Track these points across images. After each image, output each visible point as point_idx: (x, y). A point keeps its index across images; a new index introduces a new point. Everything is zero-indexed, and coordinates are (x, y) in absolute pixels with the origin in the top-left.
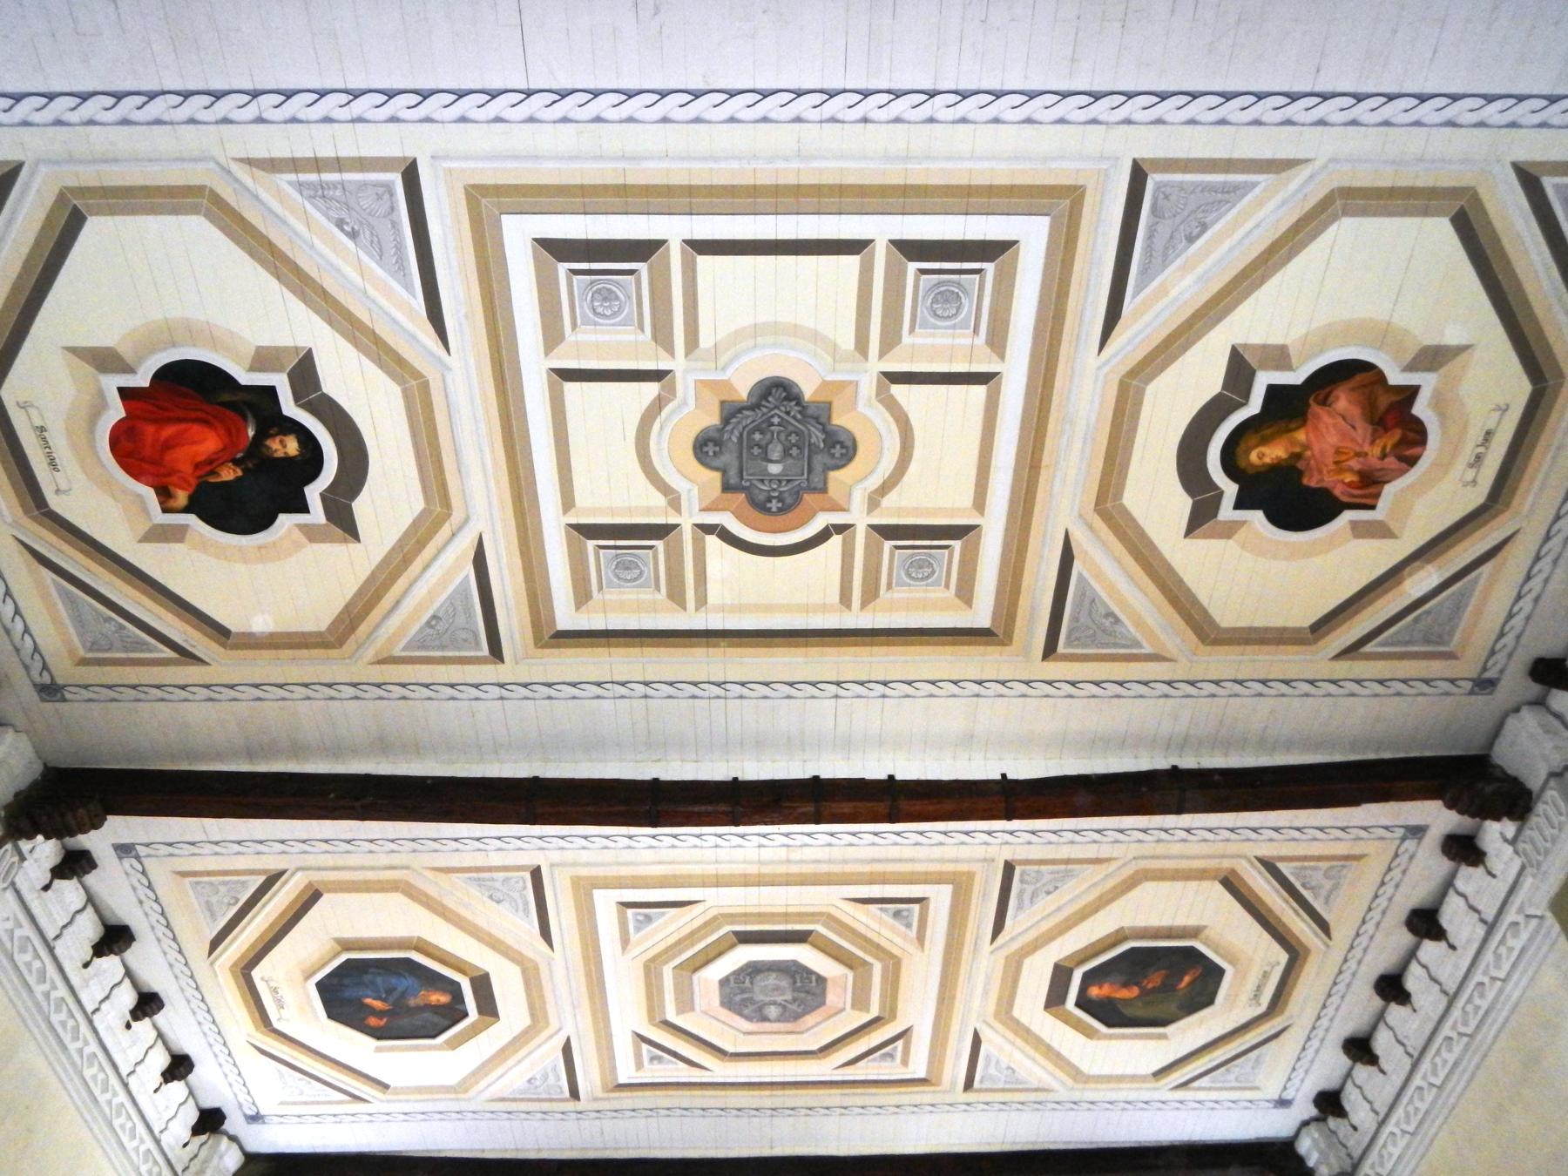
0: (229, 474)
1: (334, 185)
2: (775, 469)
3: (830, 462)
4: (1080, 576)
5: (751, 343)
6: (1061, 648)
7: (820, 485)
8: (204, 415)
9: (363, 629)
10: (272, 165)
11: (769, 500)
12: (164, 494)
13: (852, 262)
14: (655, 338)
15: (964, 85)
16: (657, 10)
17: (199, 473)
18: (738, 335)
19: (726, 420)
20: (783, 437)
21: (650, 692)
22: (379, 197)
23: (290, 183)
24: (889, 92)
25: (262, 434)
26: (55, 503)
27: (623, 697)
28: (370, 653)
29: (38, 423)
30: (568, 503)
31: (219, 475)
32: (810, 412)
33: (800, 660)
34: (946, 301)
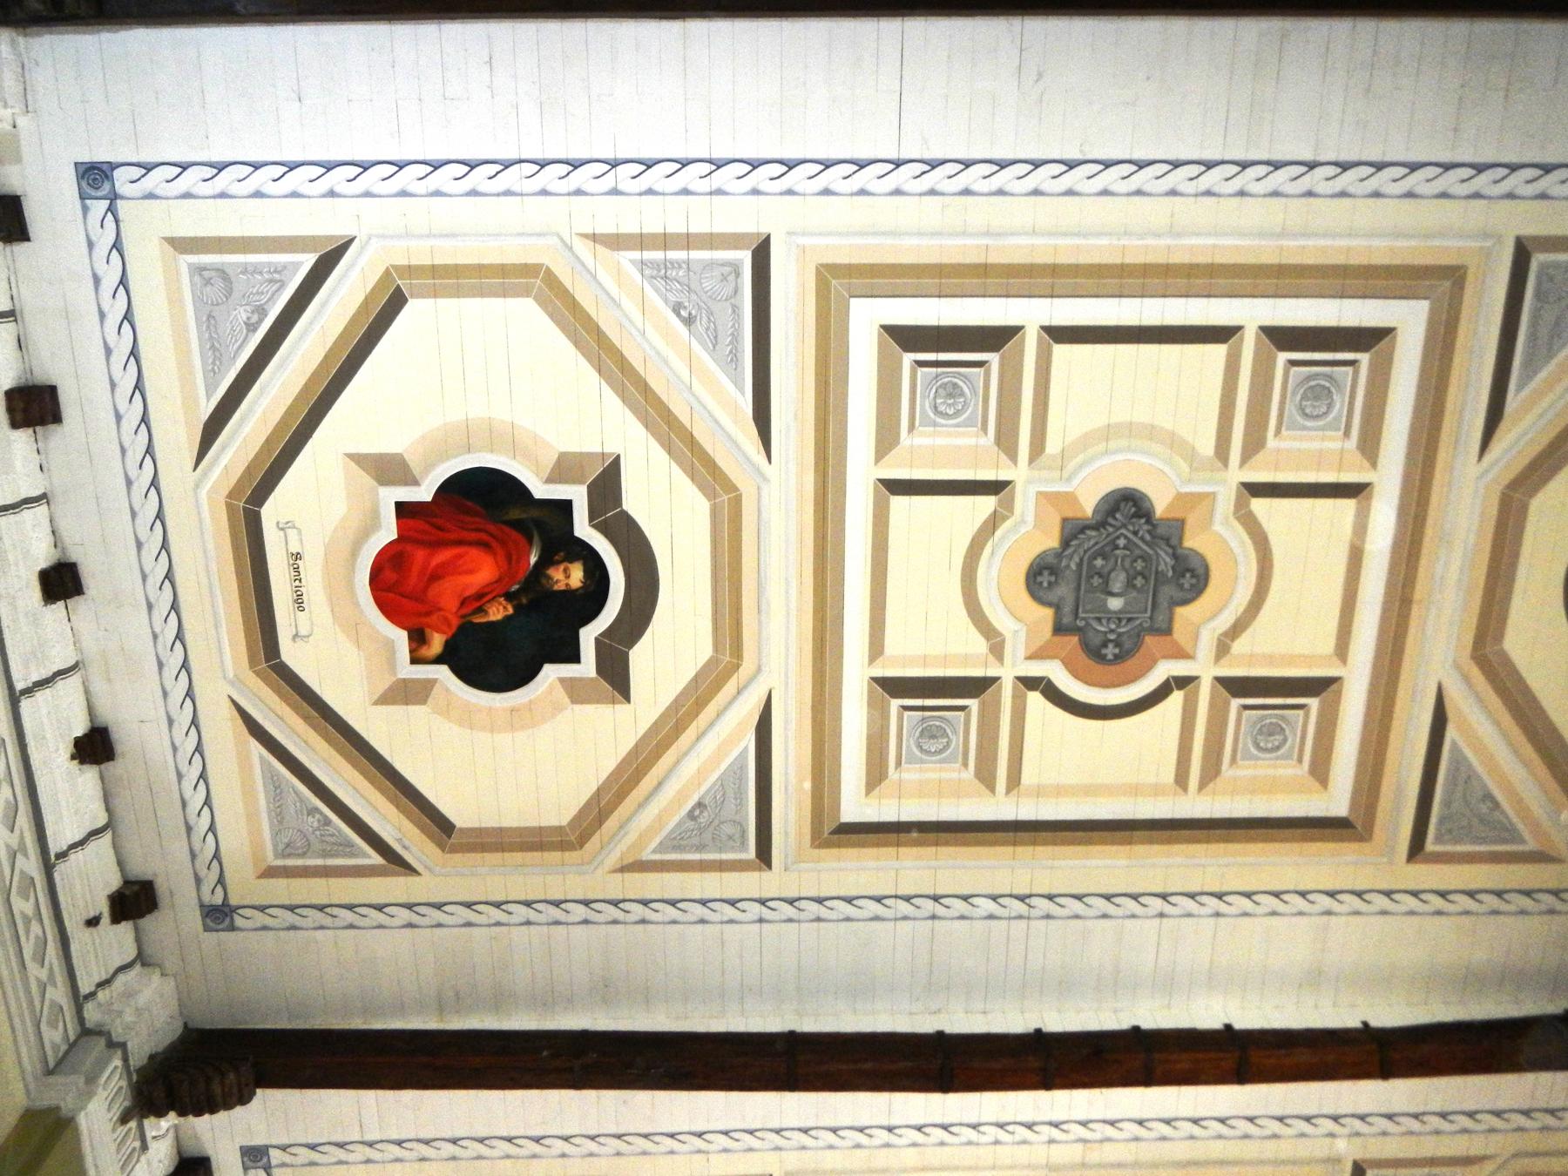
0: (498, 612)
1: (677, 265)
2: (1115, 604)
3: (1179, 595)
4: (1454, 743)
5: (1102, 447)
6: (1431, 846)
7: (1164, 626)
8: (484, 536)
9: (611, 823)
10: (616, 242)
11: (1105, 645)
12: (418, 638)
13: (1216, 353)
14: (998, 441)
15: (1344, 157)
16: (1040, 75)
17: (464, 611)
18: (1086, 441)
19: (1065, 543)
20: (1127, 564)
21: (940, 910)
22: (724, 278)
23: (633, 262)
24: (1268, 163)
25: (546, 561)
26: (290, 654)
27: (905, 918)
28: (613, 858)
29: (294, 549)
30: (876, 648)
31: (486, 613)
32: (1160, 531)
33: (1124, 862)
34: (1317, 398)
